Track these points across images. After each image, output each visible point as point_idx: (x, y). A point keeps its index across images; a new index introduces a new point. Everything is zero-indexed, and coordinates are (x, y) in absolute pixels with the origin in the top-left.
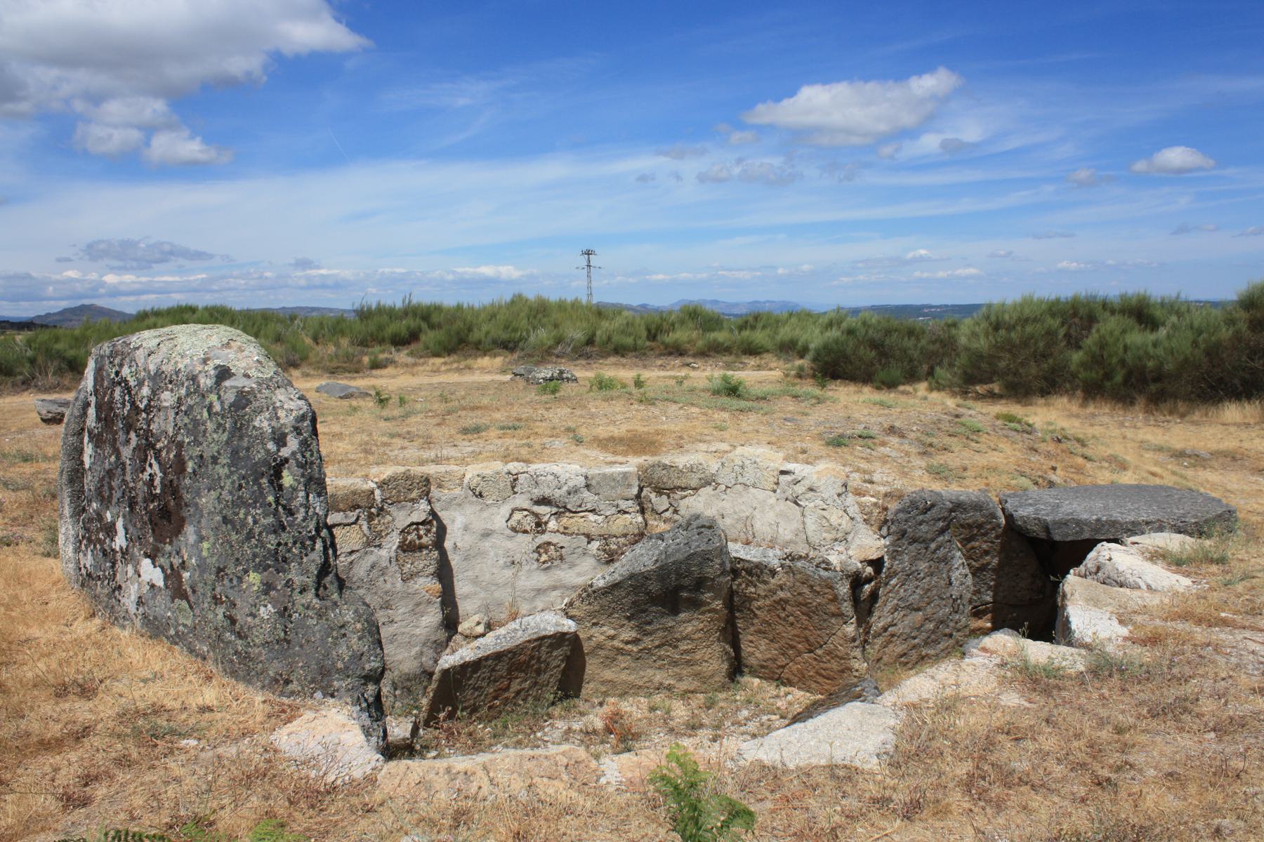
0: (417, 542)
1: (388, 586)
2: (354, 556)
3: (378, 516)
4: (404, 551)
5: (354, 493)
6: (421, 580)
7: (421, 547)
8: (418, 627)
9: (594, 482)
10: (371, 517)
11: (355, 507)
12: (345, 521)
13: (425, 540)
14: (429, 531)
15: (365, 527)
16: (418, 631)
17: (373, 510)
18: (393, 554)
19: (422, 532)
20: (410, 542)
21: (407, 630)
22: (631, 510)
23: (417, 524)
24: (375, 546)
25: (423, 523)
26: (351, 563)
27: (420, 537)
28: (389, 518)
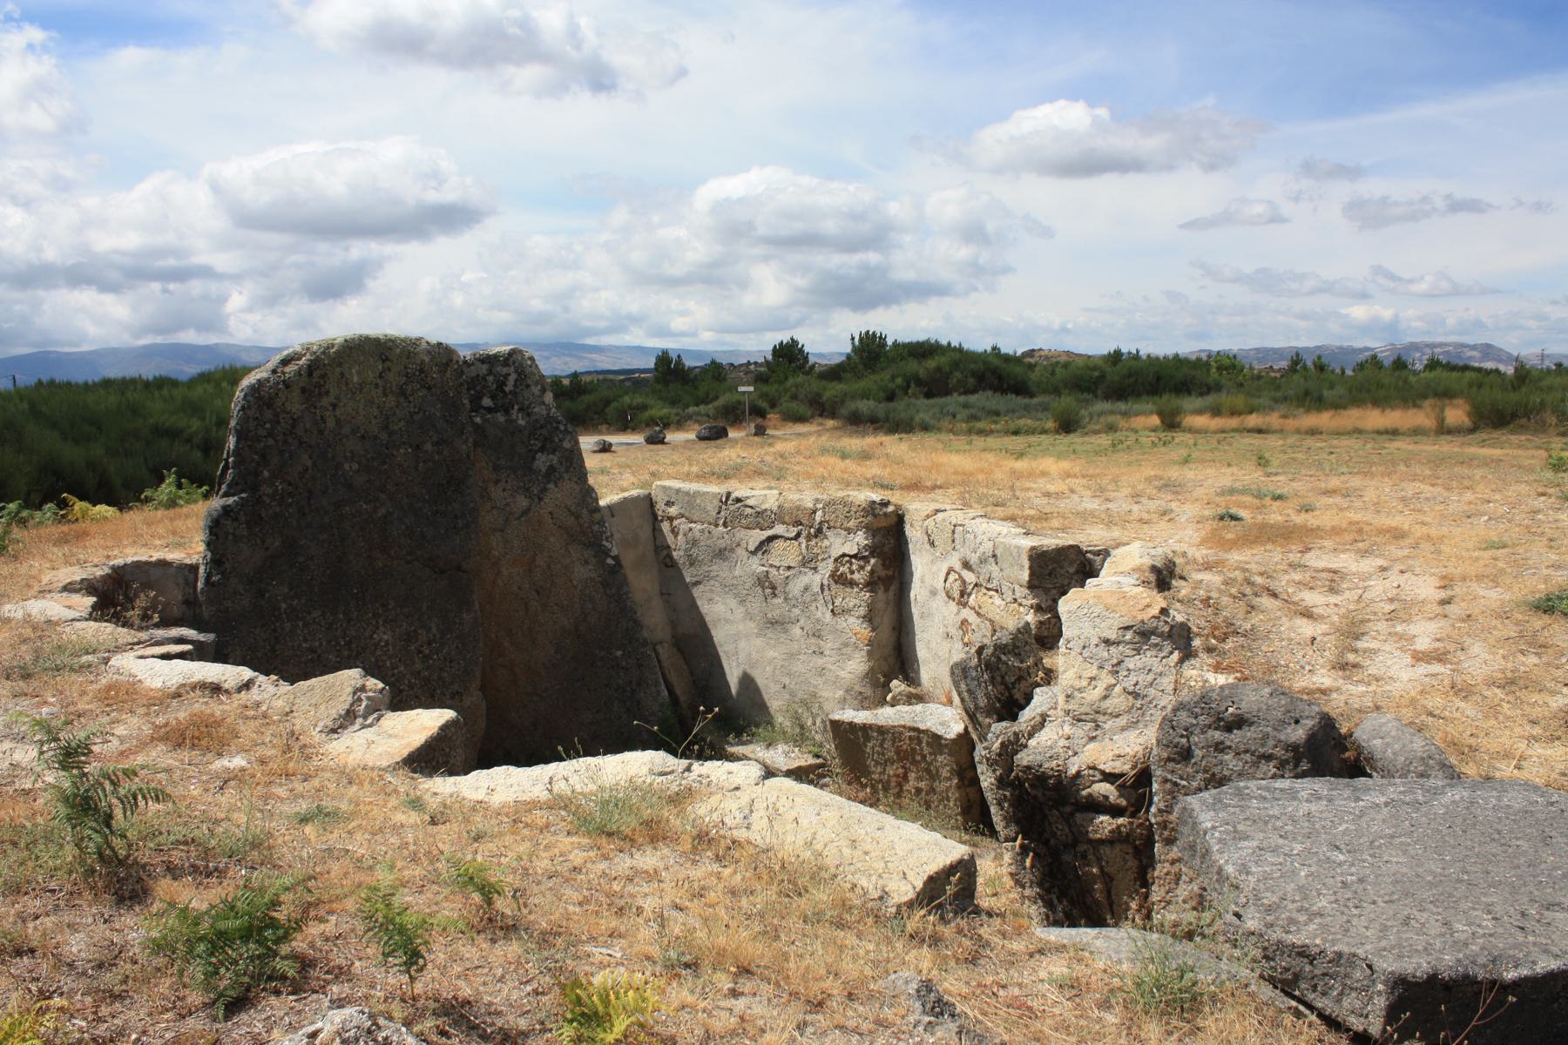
0: (849, 576)
1: (819, 614)
2: (791, 572)
3: (816, 536)
4: (836, 582)
5: (798, 508)
6: (852, 620)
7: (852, 583)
8: (843, 670)
9: (998, 553)
10: (809, 538)
11: (798, 523)
12: (786, 535)
13: (856, 576)
14: (862, 568)
15: (803, 546)
16: (842, 674)
17: (812, 530)
18: (826, 582)
19: (854, 567)
20: (842, 574)
21: (833, 668)
22: (1024, 602)
23: (851, 557)
24: (811, 568)
25: (855, 556)
26: (787, 578)
27: (852, 572)
28: (826, 543)
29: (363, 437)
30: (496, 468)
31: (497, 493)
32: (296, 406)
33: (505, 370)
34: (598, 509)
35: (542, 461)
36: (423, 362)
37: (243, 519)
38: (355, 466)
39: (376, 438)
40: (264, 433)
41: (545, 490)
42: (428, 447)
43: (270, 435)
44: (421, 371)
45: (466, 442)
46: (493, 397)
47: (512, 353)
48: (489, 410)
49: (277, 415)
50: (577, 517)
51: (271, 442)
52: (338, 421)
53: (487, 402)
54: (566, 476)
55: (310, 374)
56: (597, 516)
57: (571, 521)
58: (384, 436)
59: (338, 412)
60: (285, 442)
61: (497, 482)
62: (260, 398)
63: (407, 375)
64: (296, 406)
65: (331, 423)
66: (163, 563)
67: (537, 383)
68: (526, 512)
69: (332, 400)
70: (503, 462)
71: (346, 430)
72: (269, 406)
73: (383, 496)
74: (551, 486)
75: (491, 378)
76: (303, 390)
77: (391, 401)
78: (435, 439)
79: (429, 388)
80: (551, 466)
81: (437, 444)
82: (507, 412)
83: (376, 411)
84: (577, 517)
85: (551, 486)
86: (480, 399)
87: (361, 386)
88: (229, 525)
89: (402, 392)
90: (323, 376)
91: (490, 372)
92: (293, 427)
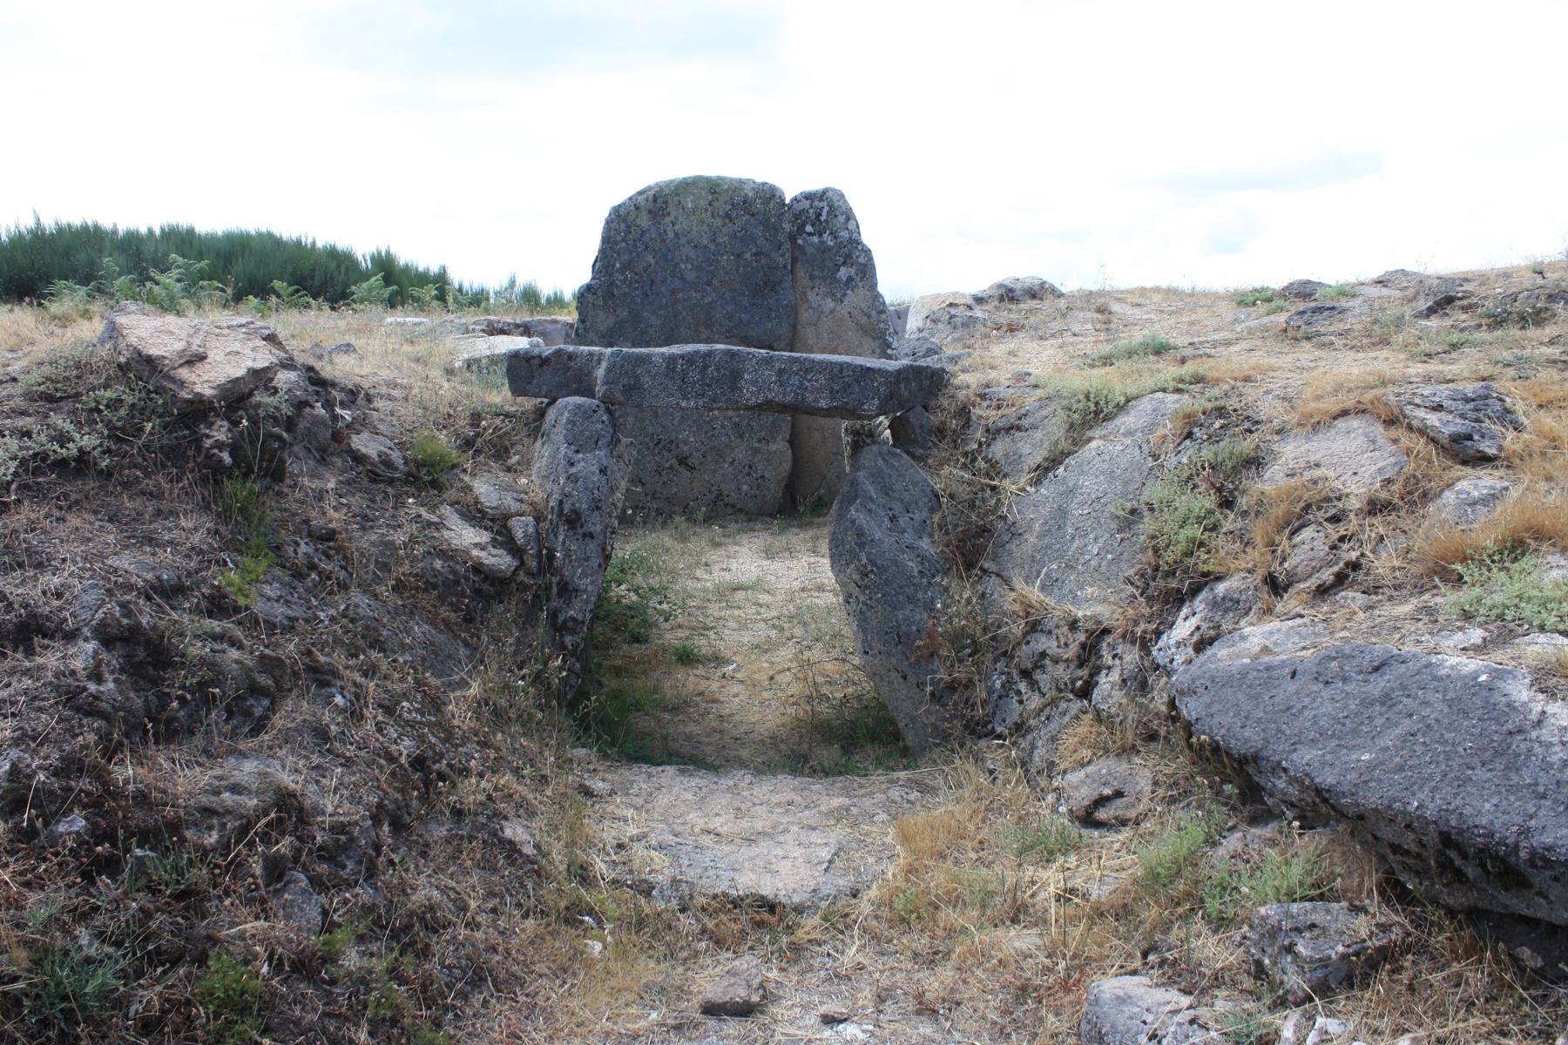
29: (696, 246)
30: (812, 278)
31: (811, 295)
32: (644, 221)
33: (821, 204)
34: (883, 312)
35: (843, 273)
36: (747, 195)
37: (600, 294)
38: (689, 266)
39: (706, 247)
40: (619, 238)
41: (845, 295)
42: (748, 256)
43: (623, 240)
44: (745, 202)
45: (783, 255)
46: (813, 225)
47: (825, 192)
48: (810, 234)
49: (628, 227)
50: (869, 317)
51: (624, 245)
52: (676, 234)
53: (809, 228)
54: (860, 284)
55: (655, 201)
56: (883, 317)
57: (864, 320)
58: (712, 247)
59: (676, 228)
60: (635, 246)
61: (813, 288)
62: (619, 216)
63: (733, 204)
64: (644, 221)
65: (671, 235)
66: (555, 322)
67: (843, 213)
68: (832, 312)
69: (671, 218)
70: (816, 273)
71: (683, 241)
72: (624, 221)
73: (709, 289)
74: (849, 292)
75: (811, 211)
76: (650, 212)
77: (718, 222)
78: (754, 251)
79: (753, 215)
80: (850, 277)
81: (755, 254)
82: (821, 235)
83: (706, 229)
84: (869, 317)
85: (849, 292)
86: (804, 226)
87: (694, 210)
88: (590, 298)
89: (728, 216)
90: (666, 202)
91: (811, 206)
92: (642, 236)
